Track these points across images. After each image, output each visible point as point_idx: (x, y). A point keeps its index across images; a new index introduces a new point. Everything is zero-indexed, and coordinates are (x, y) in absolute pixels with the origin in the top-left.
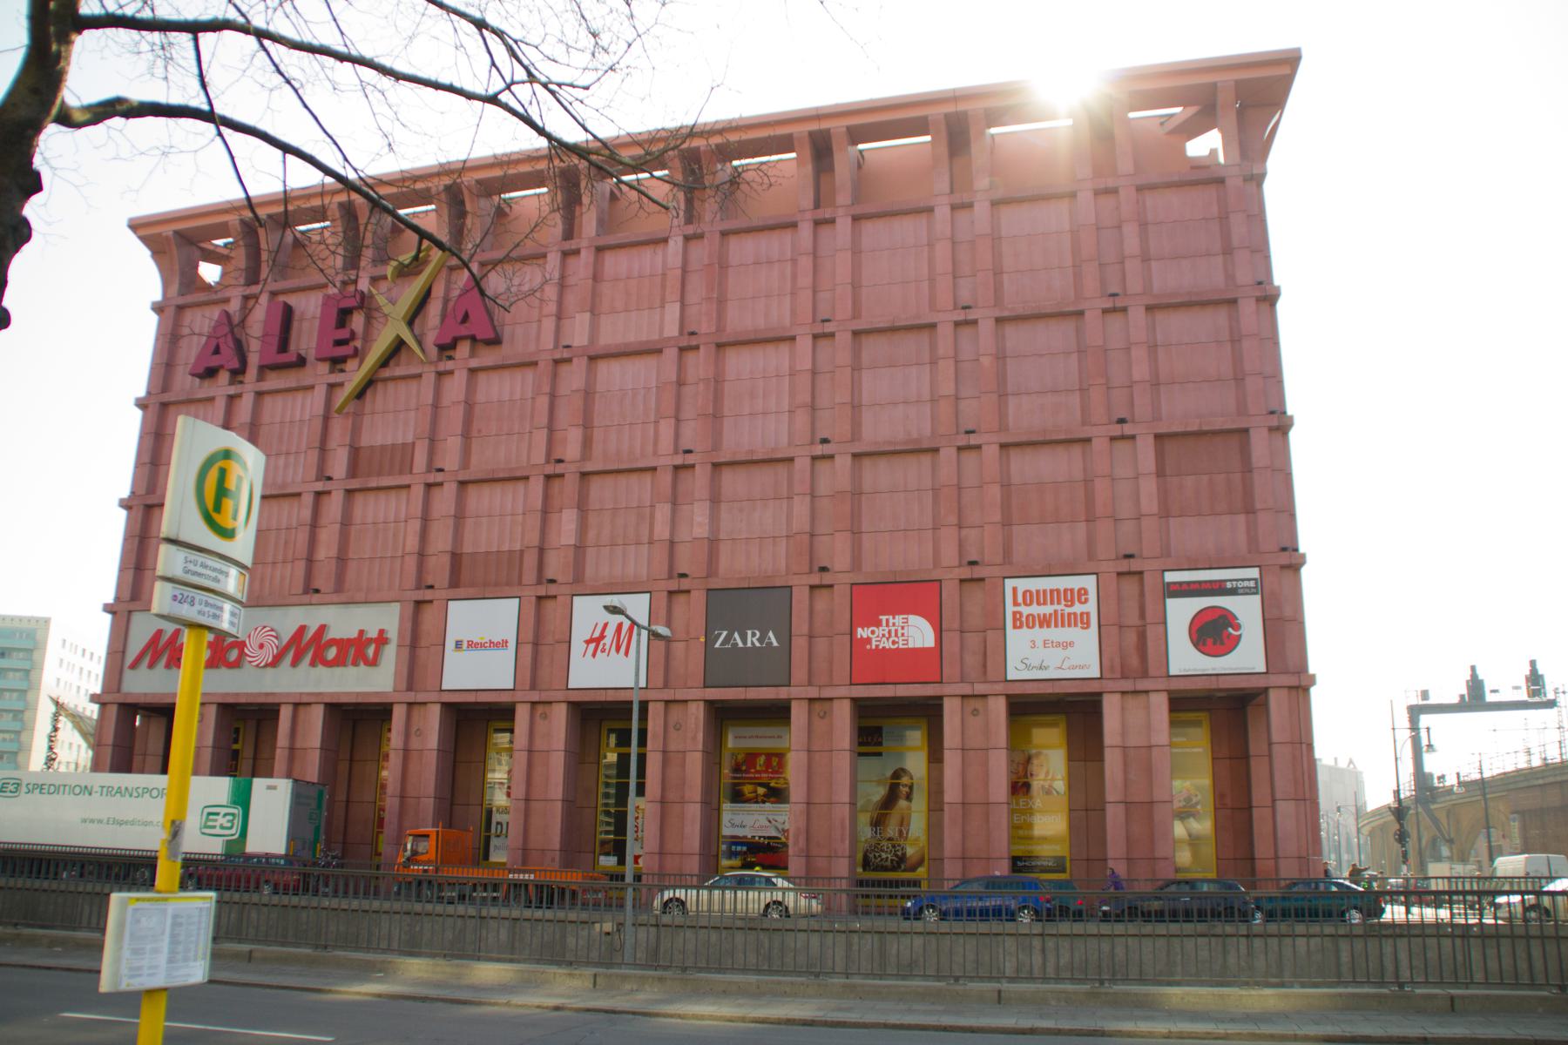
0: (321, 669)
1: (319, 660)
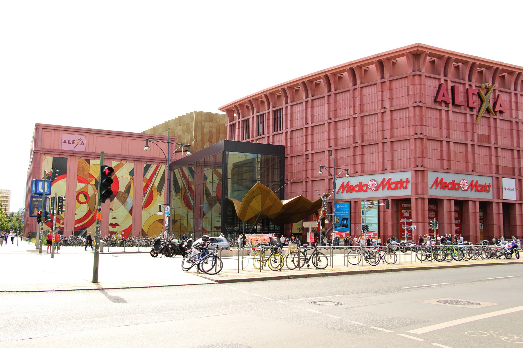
0: (390, 190)
1: (390, 188)
